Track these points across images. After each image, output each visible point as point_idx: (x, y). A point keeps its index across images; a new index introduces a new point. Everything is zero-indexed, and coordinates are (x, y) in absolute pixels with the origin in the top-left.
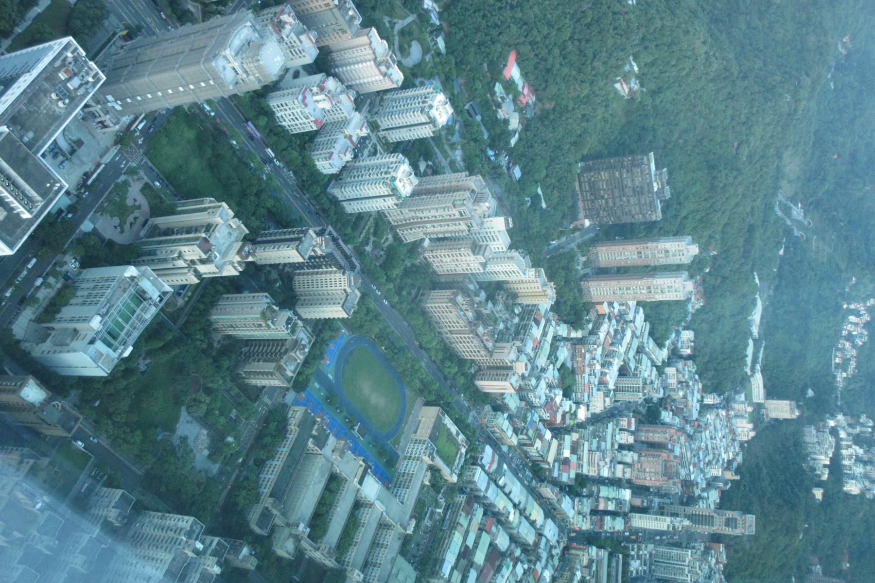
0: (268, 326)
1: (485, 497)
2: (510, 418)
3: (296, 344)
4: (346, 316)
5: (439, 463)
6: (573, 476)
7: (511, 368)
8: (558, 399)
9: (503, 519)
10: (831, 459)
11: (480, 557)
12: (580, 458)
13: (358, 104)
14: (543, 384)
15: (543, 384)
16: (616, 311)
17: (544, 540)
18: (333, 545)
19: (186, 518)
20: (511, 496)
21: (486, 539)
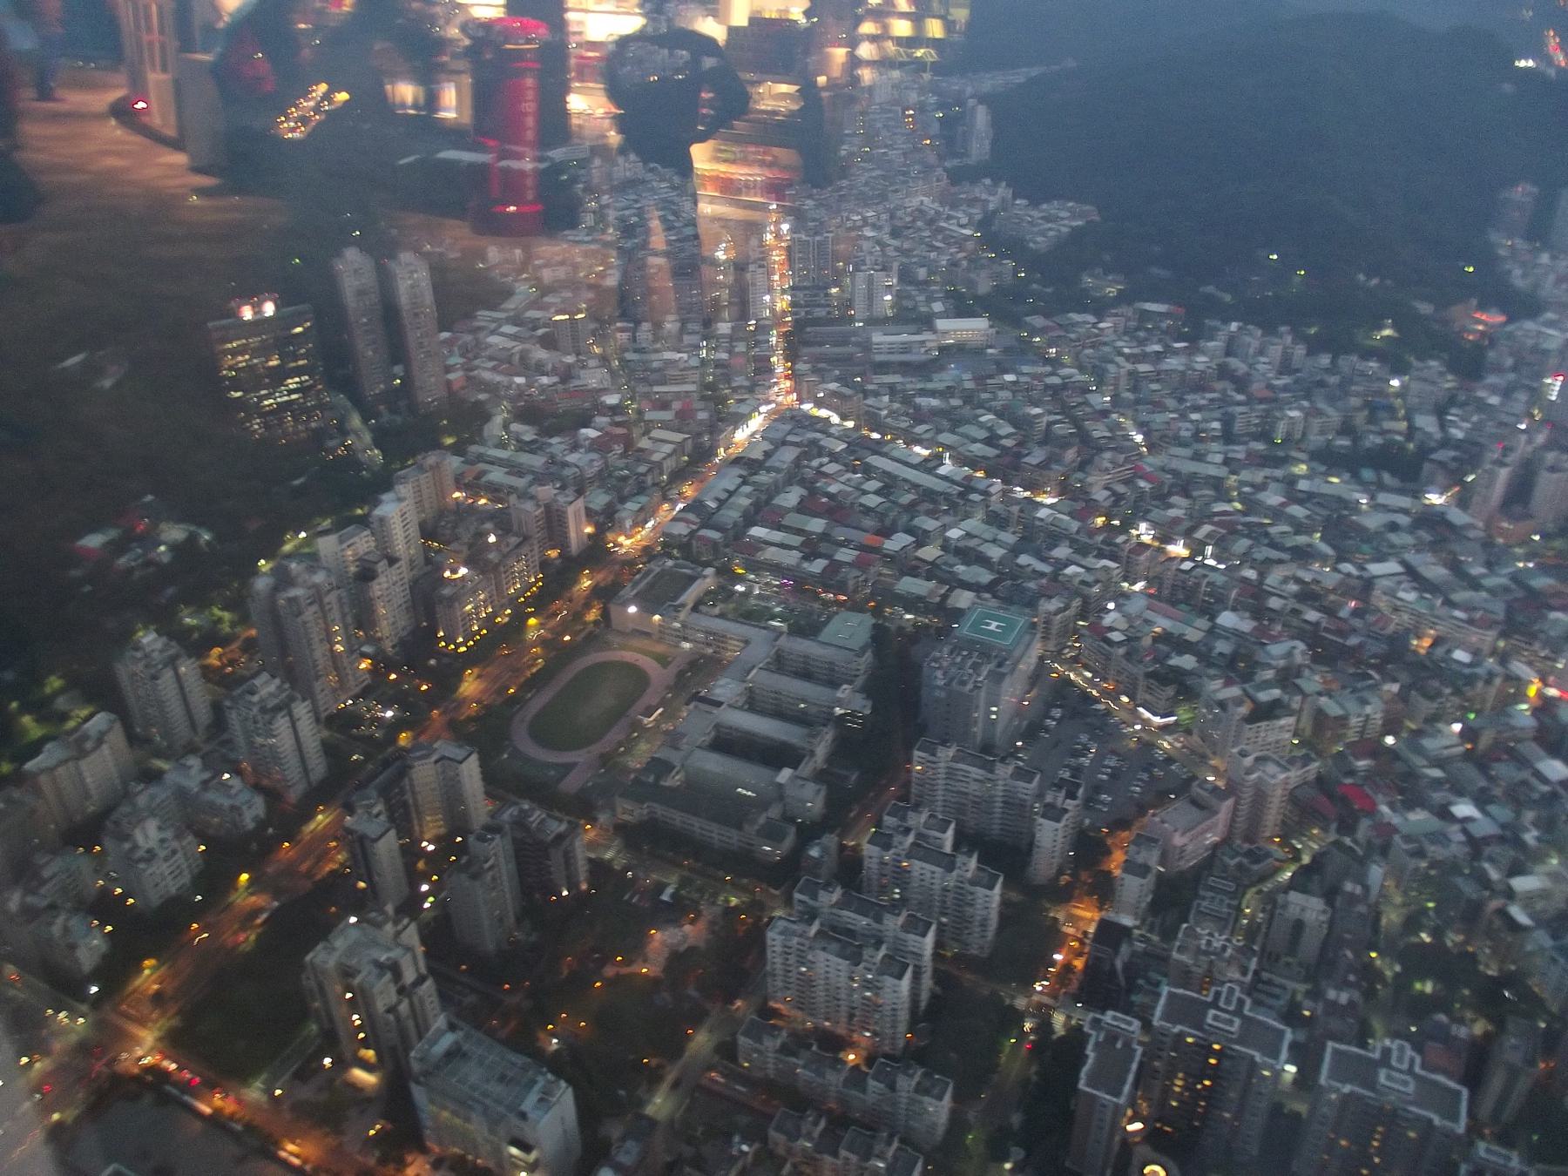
0: (491, 868)
1: (735, 524)
2: (623, 500)
3: (520, 823)
4: (474, 757)
5: (690, 595)
6: (701, 405)
7: (548, 507)
8: (591, 433)
9: (764, 497)
10: (661, 46)
11: (817, 525)
12: (678, 395)
13: (151, 777)
14: (572, 458)
15: (572, 458)
16: (461, 360)
17: (790, 438)
18: (805, 731)
19: (769, 942)
20: (732, 488)
21: (792, 519)
